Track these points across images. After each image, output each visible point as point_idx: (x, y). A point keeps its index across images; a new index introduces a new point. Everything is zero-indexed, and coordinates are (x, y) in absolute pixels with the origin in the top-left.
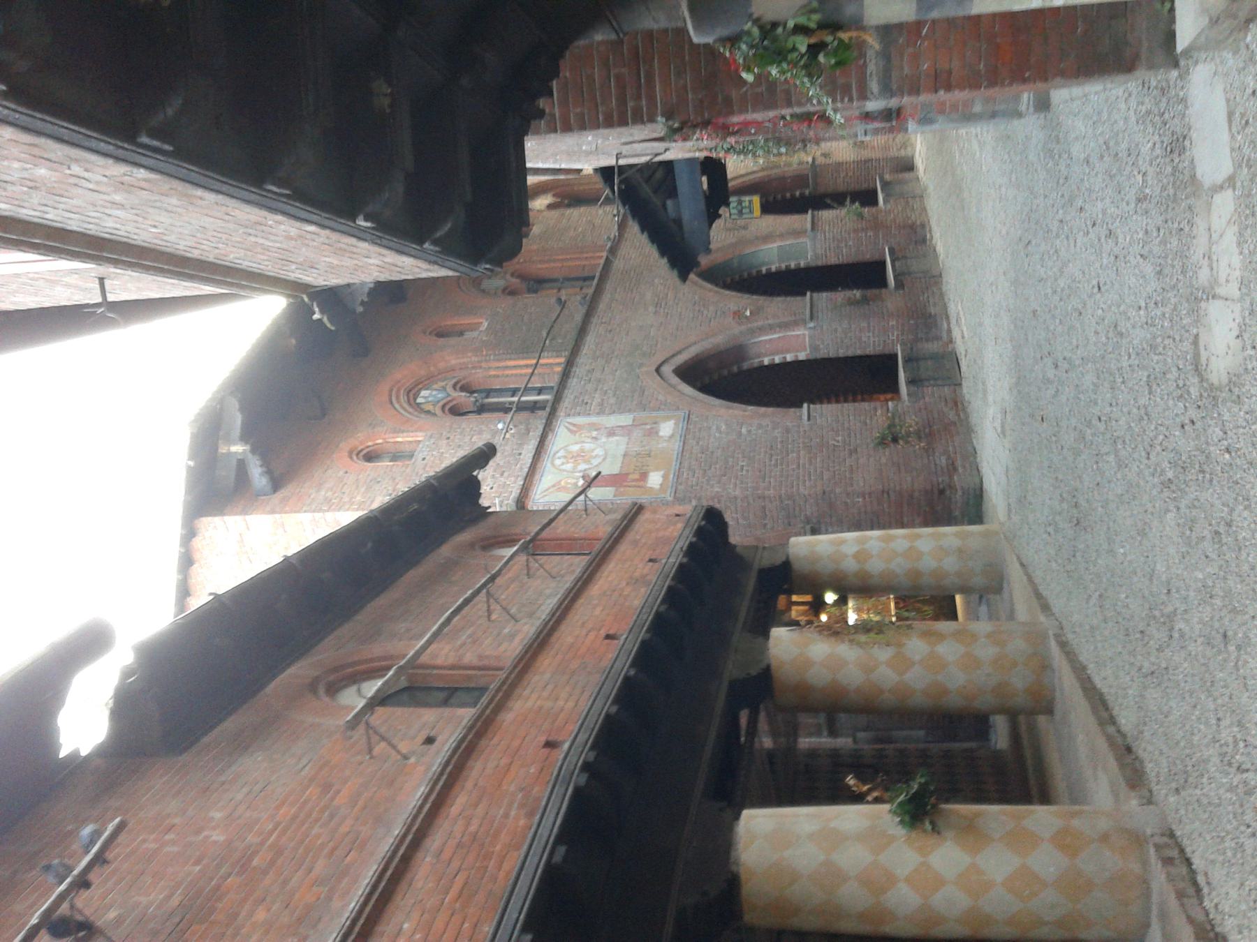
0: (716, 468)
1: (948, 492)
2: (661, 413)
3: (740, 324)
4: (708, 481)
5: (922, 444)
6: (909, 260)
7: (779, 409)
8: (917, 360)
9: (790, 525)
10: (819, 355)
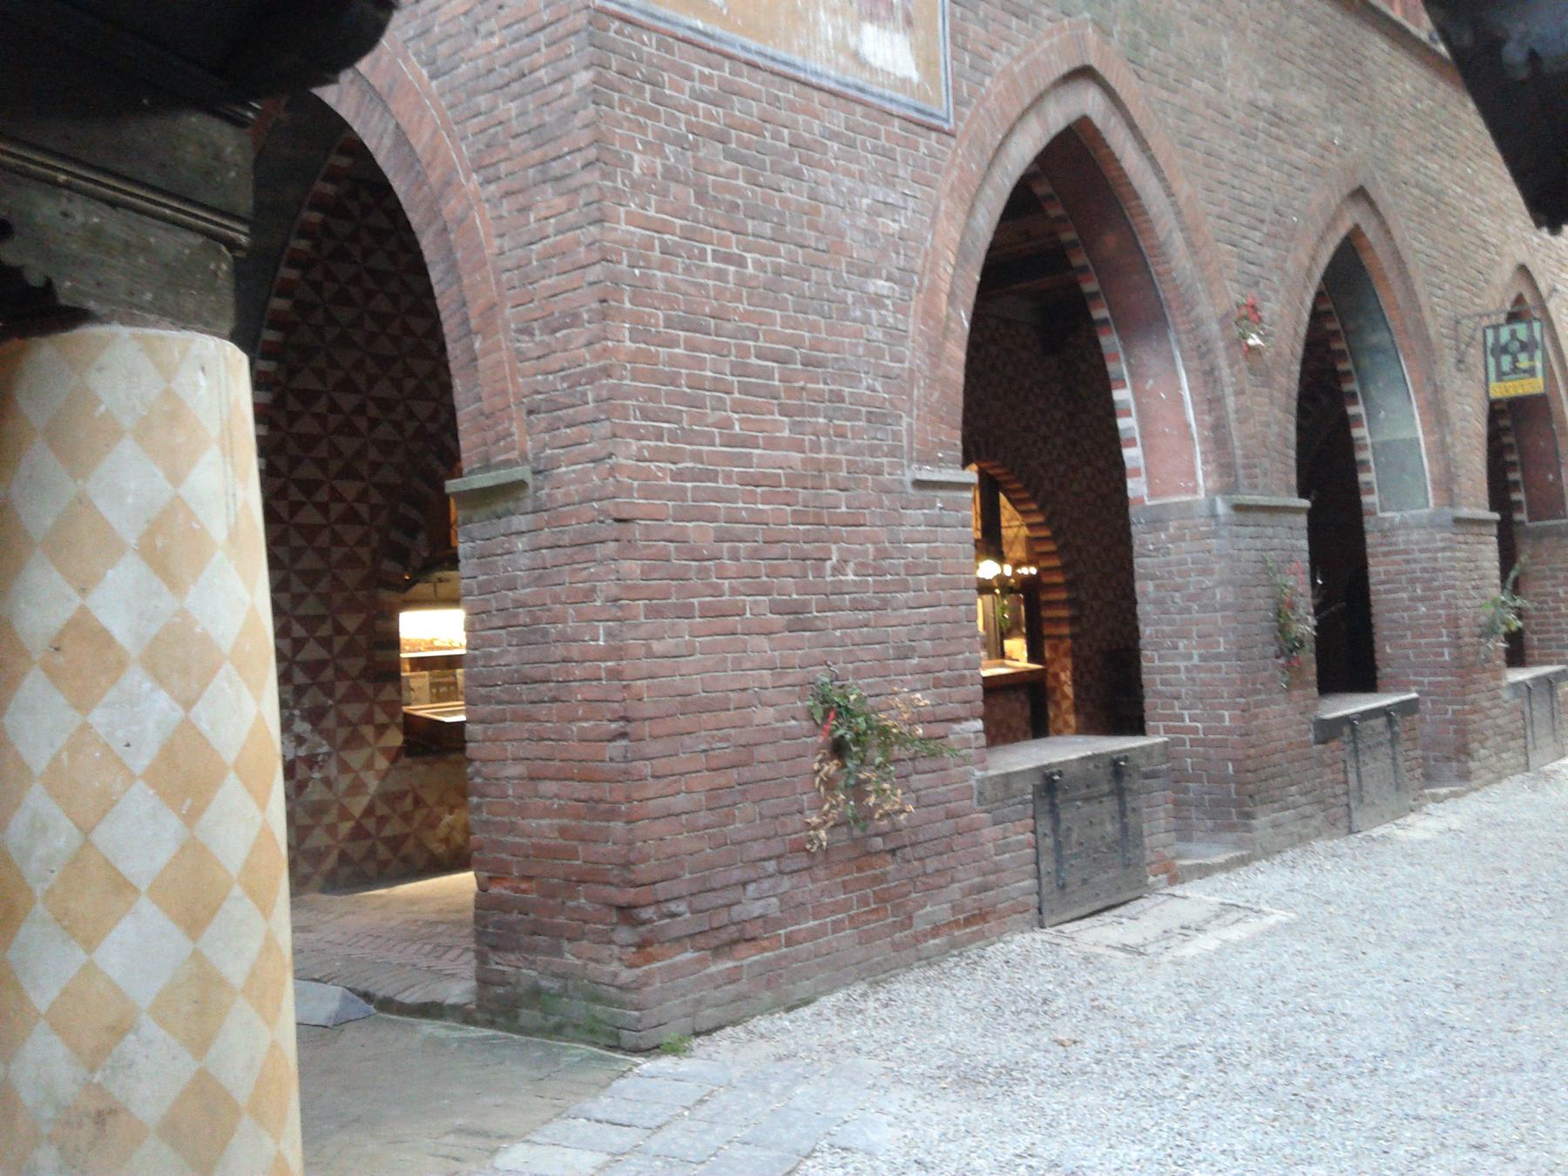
0: (733, 174)
1: (624, 934)
2: (944, 51)
3: (1223, 320)
4: (678, 141)
5: (822, 834)
6: (1385, 749)
7: (959, 400)
8: (1120, 793)
9: (530, 412)
10: (1141, 535)
